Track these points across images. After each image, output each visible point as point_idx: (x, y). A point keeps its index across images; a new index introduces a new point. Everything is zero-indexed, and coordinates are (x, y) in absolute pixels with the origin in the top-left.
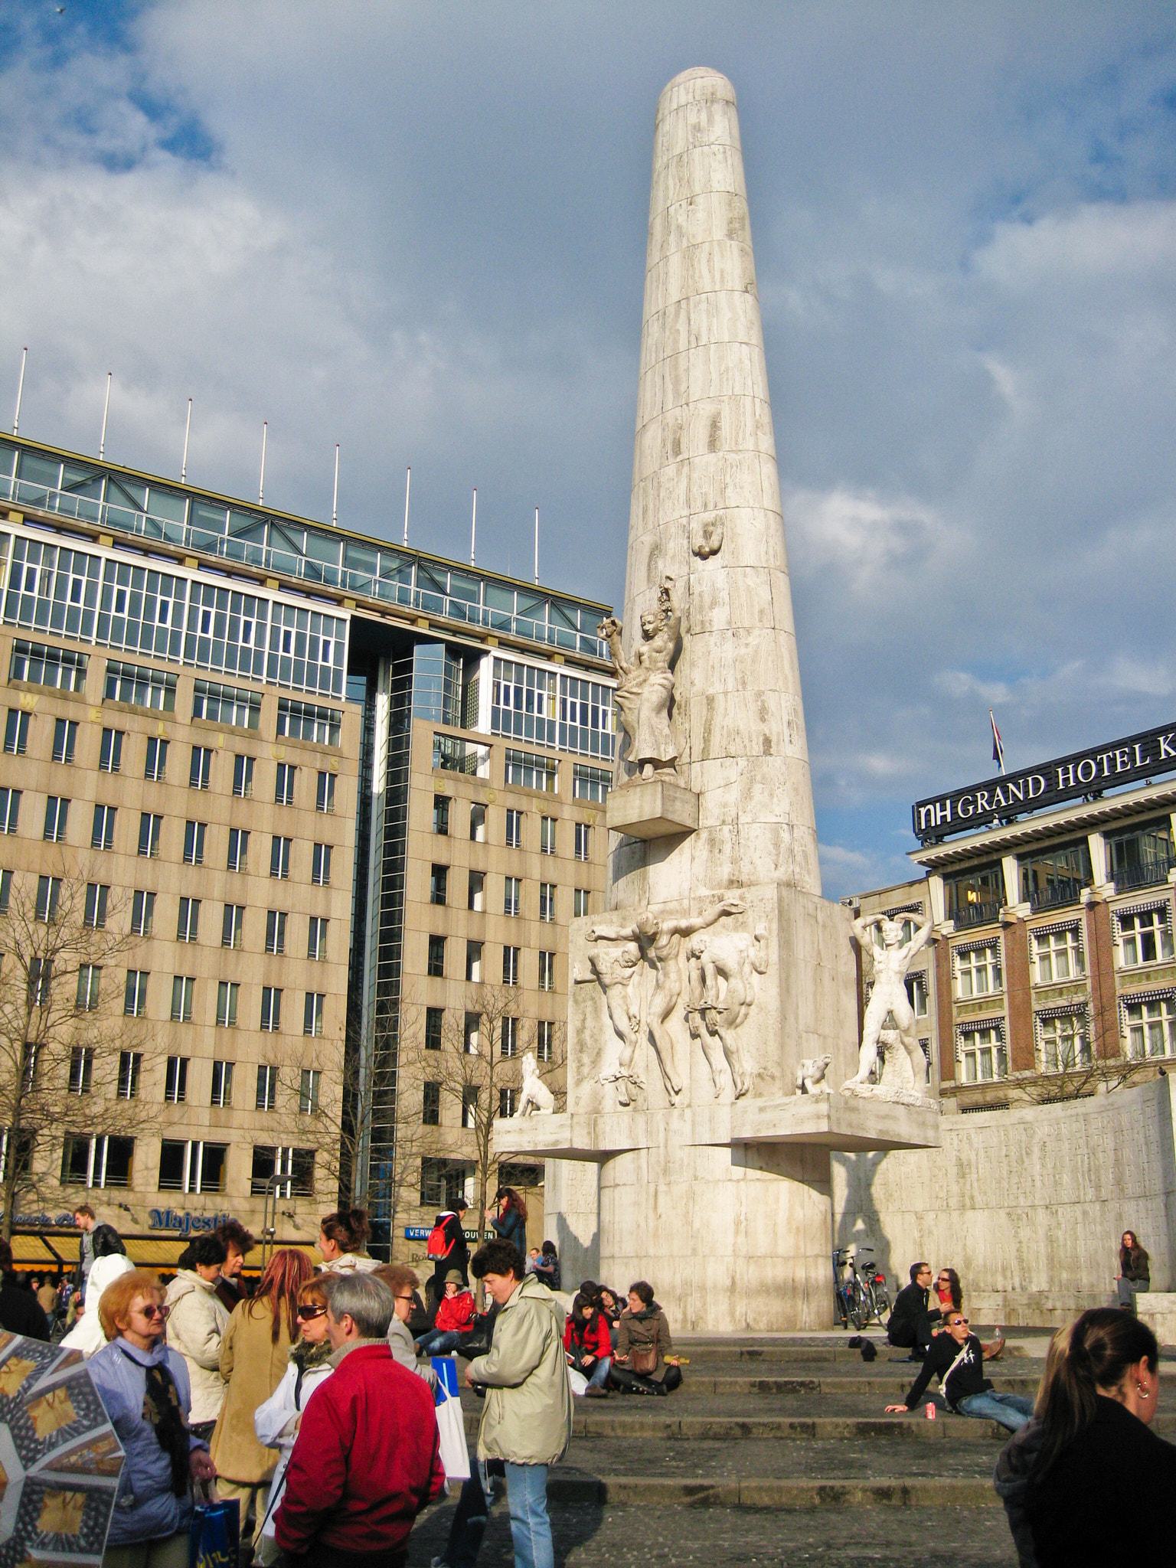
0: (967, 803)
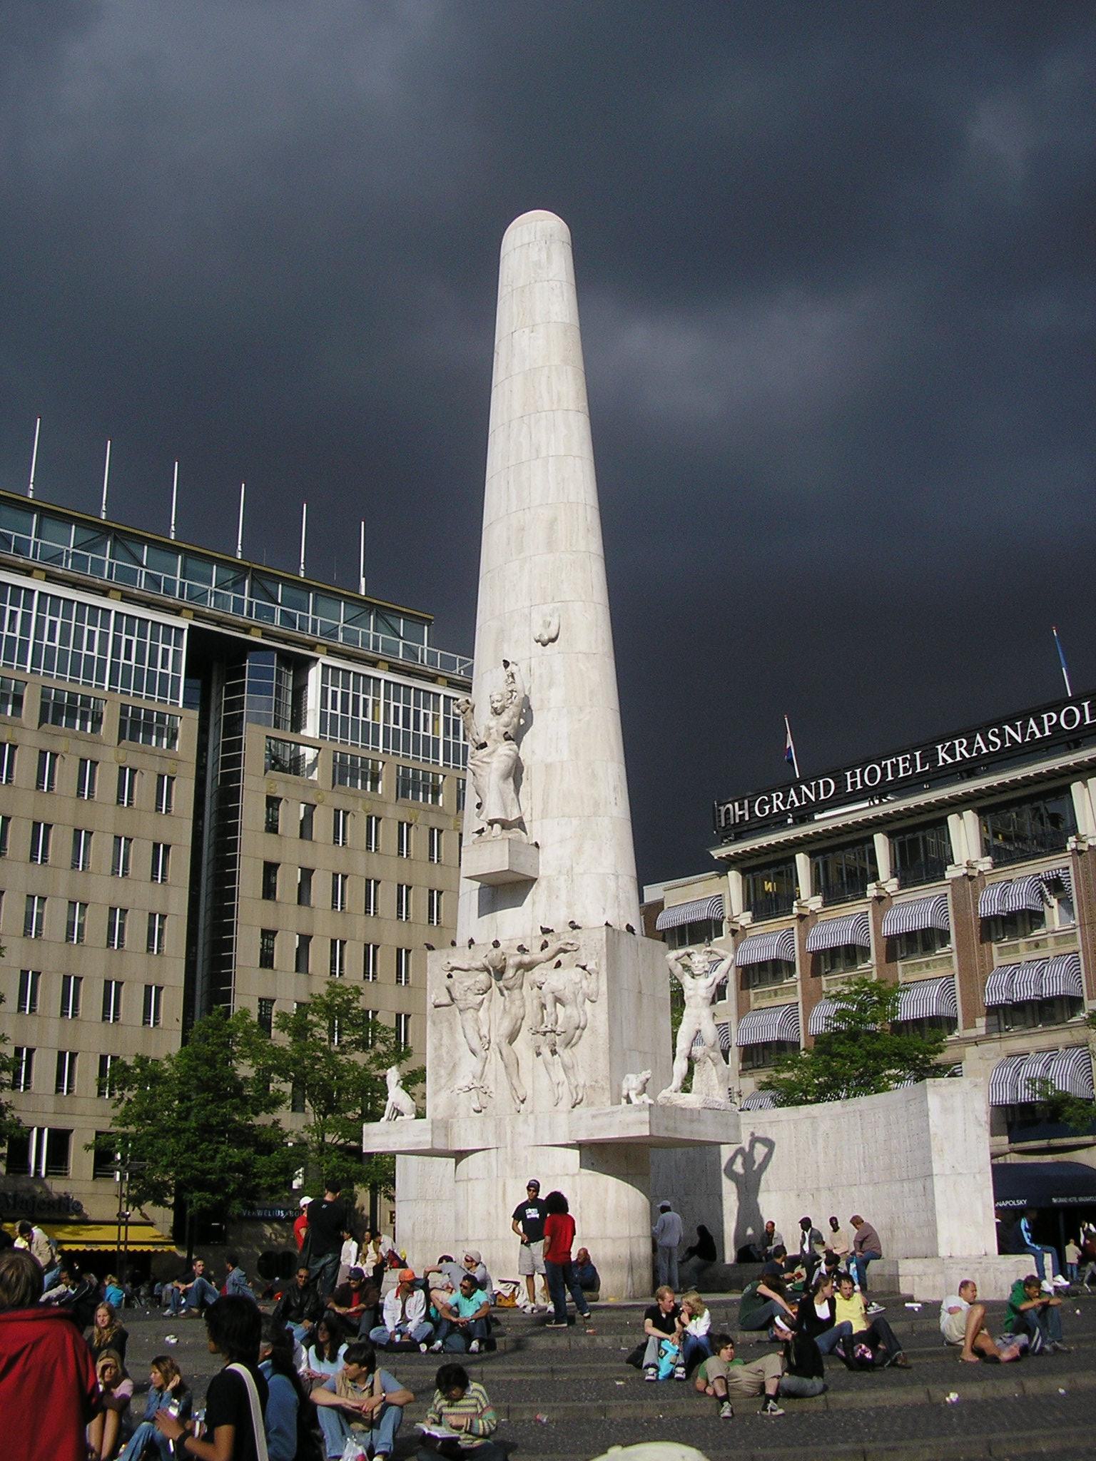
0: (763, 803)
